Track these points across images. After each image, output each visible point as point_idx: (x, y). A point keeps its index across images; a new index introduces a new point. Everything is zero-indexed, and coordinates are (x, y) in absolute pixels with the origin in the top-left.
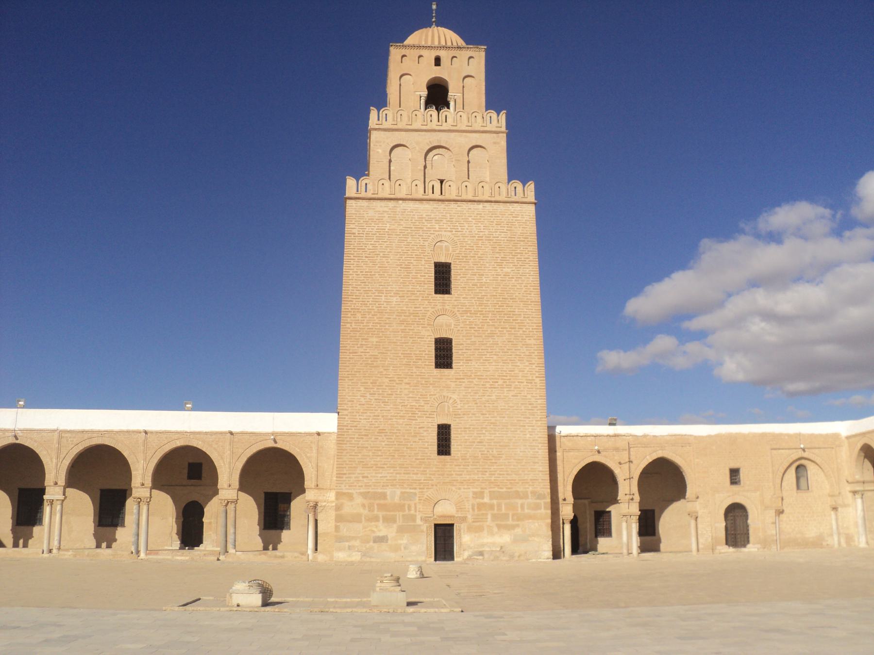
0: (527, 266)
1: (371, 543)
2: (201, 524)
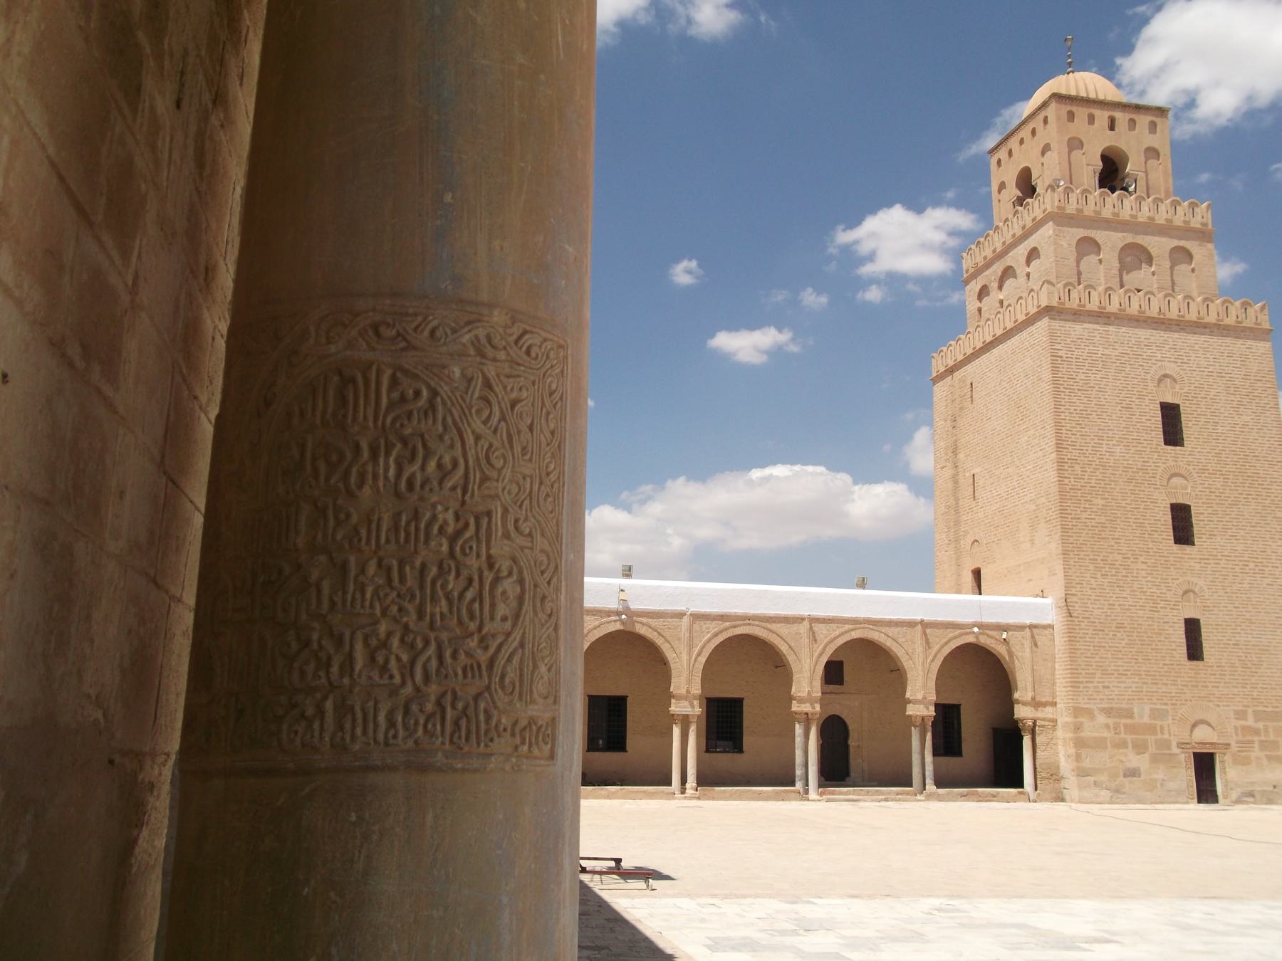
0: (1268, 414)
1: (1121, 778)
2: (847, 746)
